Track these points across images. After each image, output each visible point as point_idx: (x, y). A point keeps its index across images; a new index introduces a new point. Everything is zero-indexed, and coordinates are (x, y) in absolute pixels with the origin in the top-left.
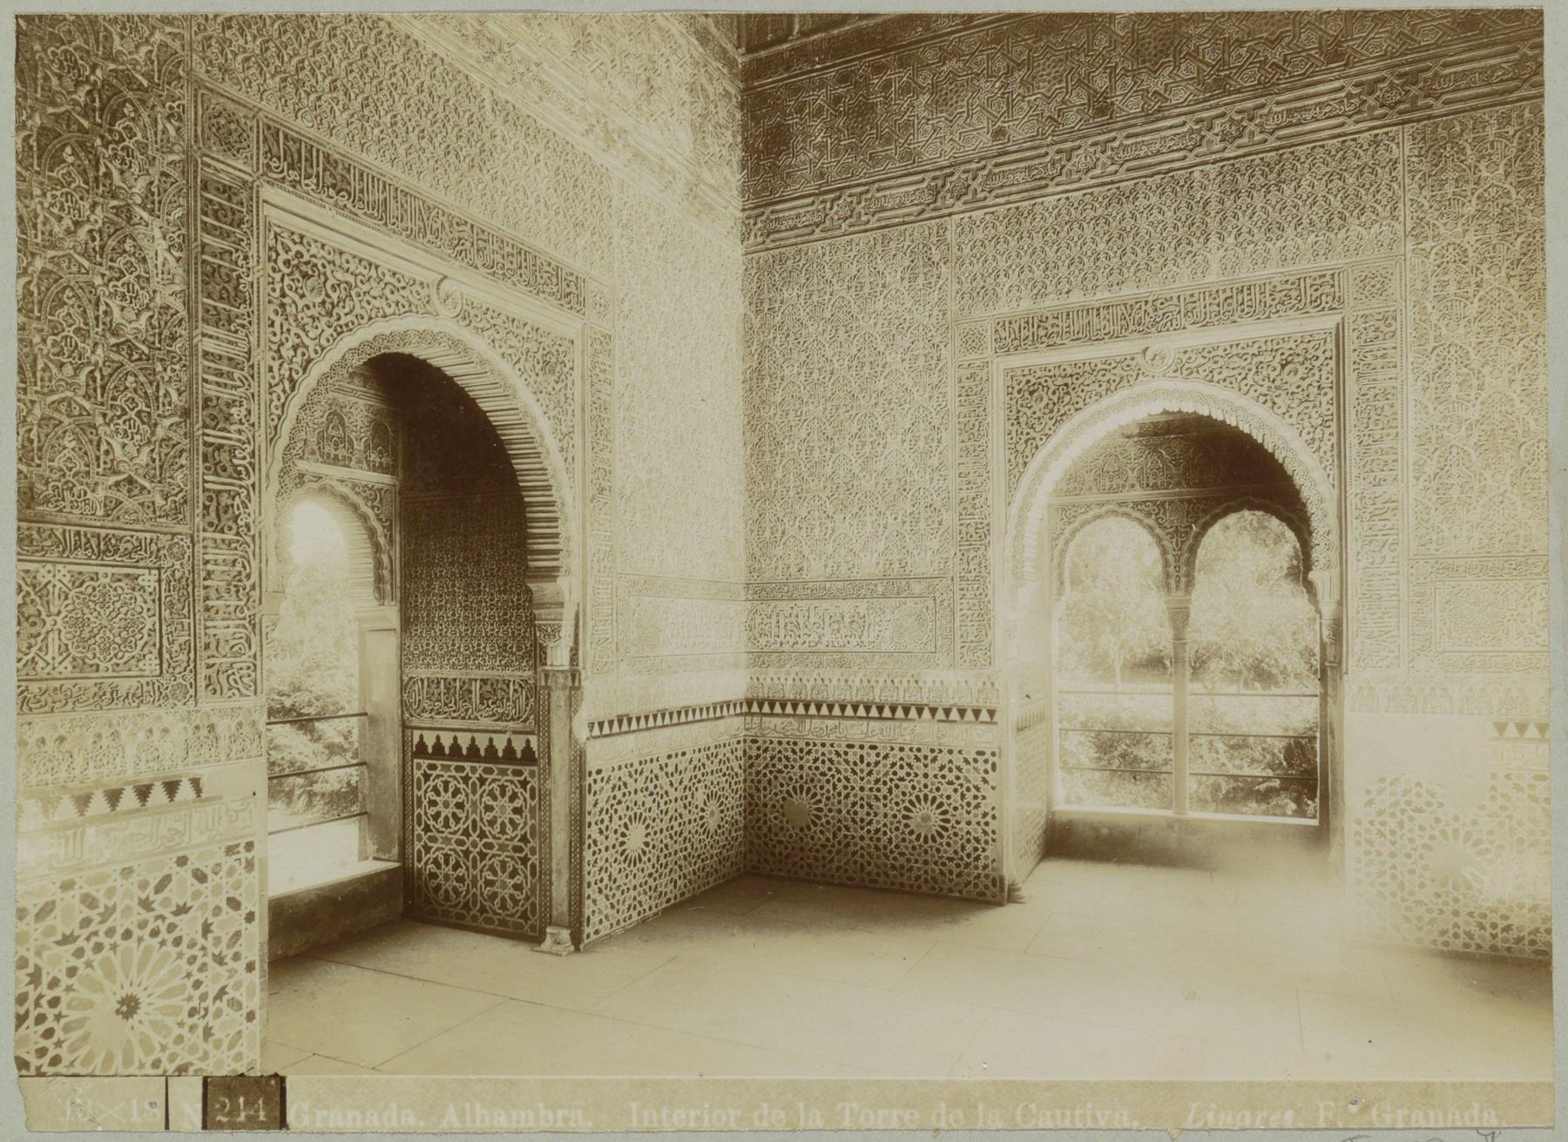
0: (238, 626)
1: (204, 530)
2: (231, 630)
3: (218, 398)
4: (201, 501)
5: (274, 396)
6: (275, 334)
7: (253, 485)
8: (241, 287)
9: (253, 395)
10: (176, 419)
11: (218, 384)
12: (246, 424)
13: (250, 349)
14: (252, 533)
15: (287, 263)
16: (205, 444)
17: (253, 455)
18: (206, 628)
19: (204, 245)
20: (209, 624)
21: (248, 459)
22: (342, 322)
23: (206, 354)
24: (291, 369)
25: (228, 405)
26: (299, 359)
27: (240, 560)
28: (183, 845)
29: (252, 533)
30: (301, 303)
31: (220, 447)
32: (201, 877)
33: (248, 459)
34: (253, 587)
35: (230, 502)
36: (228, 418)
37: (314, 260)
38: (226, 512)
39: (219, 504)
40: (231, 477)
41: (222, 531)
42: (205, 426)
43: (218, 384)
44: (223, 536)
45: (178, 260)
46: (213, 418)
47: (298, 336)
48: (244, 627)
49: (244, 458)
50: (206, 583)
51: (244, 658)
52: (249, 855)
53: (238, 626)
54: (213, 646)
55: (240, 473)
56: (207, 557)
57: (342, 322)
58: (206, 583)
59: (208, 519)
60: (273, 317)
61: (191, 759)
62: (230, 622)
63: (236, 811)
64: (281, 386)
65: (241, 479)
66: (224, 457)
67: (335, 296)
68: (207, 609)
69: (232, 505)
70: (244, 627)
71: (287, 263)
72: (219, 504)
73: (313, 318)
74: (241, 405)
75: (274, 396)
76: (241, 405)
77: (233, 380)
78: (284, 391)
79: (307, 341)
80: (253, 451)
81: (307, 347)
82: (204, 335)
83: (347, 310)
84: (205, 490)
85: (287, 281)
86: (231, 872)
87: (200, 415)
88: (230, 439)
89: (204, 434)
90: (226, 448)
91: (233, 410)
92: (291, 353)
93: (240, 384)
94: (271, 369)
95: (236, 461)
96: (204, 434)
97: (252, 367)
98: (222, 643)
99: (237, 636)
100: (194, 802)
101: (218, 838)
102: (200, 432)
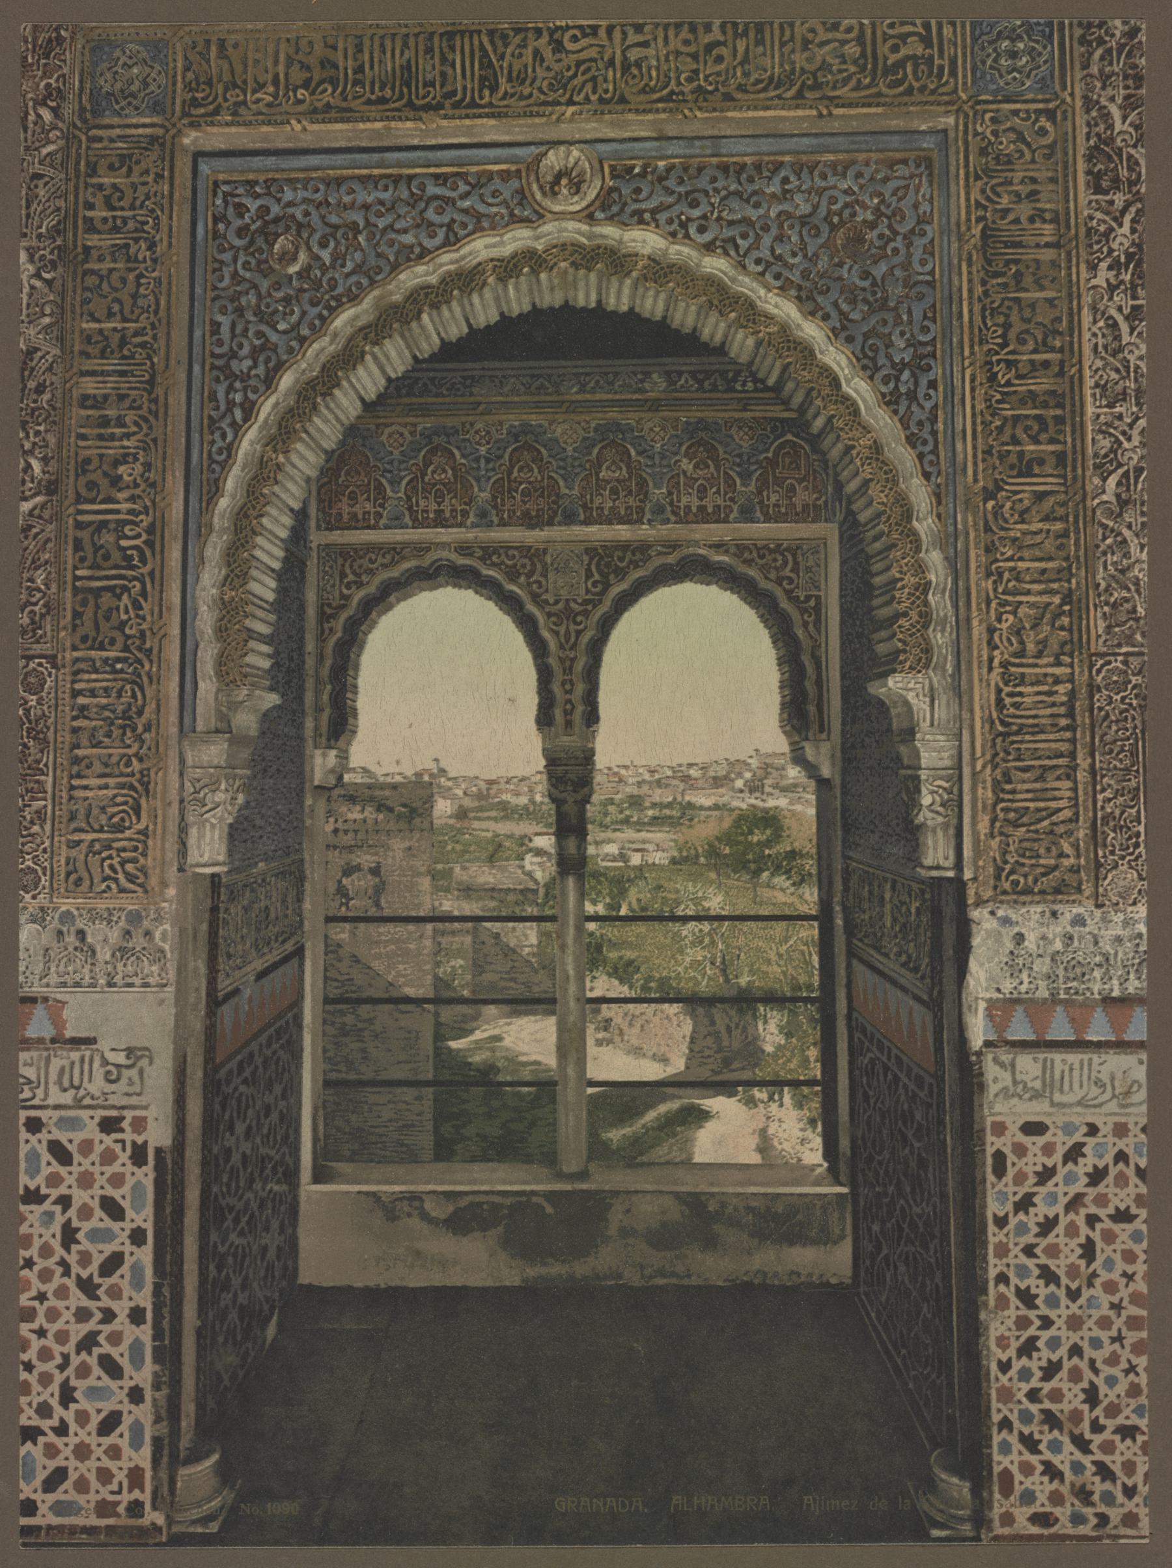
0: (122, 786)
1: (75, 648)
2: (110, 793)
3: (101, 456)
4: (69, 606)
5: (217, 435)
6: (220, 343)
7: (152, 574)
8: (142, 290)
9: (155, 440)
10: (39, 499)
11: (101, 437)
12: (143, 486)
13: (153, 377)
14: (148, 645)
15: (241, 232)
16: (79, 525)
17: (151, 530)
18: (72, 788)
19: (87, 250)
20: (75, 782)
21: (144, 537)
22: (340, 290)
23: (84, 399)
24: (245, 389)
25: (116, 463)
26: (261, 370)
27: (128, 687)
28: (36, 1102)
29: (148, 645)
30: (265, 285)
31: (103, 524)
32: (60, 1153)
33: (144, 537)
34: (147, 728)
35: (115, 603)
36: (116, 481)
37: (290, 210)
38: (108, 619)
39: (97, 607)
40: (116, 567)
41: (102, 648)
42: (79, 499)
43: (101, 437)
44: (105, 654)
45: (49, 283)
46: (91, 485)
47: (260, 334)
48: (132, 787)
49: (138, 536)
50: (75, 724)
51: (128, 833)
52: (140, 1140)
53: (122, 786)
54: (81, 815)
55: (131, 558)
56: (77, 686)
57: (340, 290)
58: (75, 724)
59: (80, 632)
60: (220, 318)
61: (53, 978)
62: (111, 781)
63: (118, 1066)
64: (228, 420)
65: (133, 567)
66: (107, 538)
67: (326, 255)
68: (76, 761)
69: (118, 608)
70: (132, 787)
71: (241, 232)
72: (97, 607)
74: (136, 459)
75: (217, 435)
76: (136, 459)
77: (124, 425)
78: (233, 424)
79: (274, 337)
80: (153, 525)
82: (83, 374)
83: (350, 266)
84: (76, 591)
86: (108, 1157)
87: (69, 485)
88: (118, 512)
89: (80, 512)
90: (112, 526)
91: (122, 469)
92: (249, 362)
93: (135, 429)
94: (213, 397)
95: (124, 543)
96: (80, 512)
97: (155, 401)
98: (95, 811)
99: (119, 799)
100: (53, 1041)
101: (87, 1101)
102: (71, 510)
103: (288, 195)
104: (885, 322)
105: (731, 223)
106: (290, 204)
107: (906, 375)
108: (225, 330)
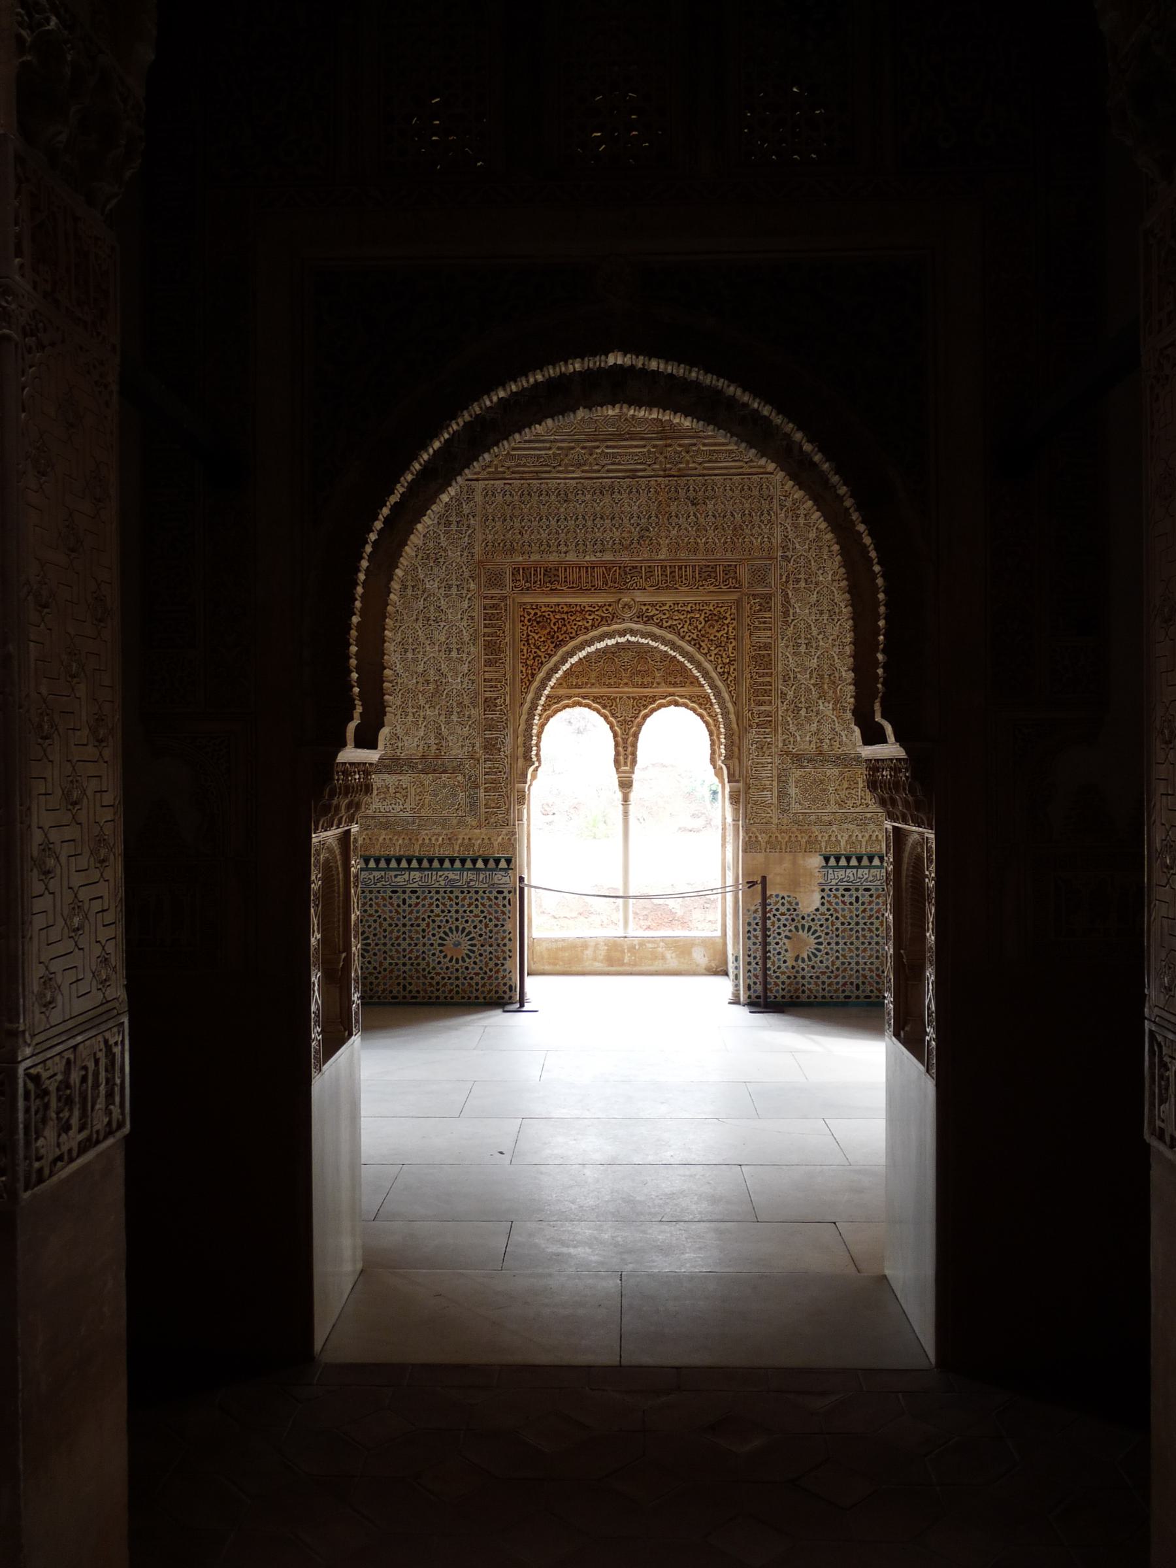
5: (524, 684)
73: (544, 642)
75: (524, 684)
78: (529, 680)
79: (540, 653)
81: (540, 657)
85: (530, 628)
103: (543, 609)
104: (720, 651)
105: (676, 620)
106: (544, 612)
107: (727, 666)
108: (525, 651)
